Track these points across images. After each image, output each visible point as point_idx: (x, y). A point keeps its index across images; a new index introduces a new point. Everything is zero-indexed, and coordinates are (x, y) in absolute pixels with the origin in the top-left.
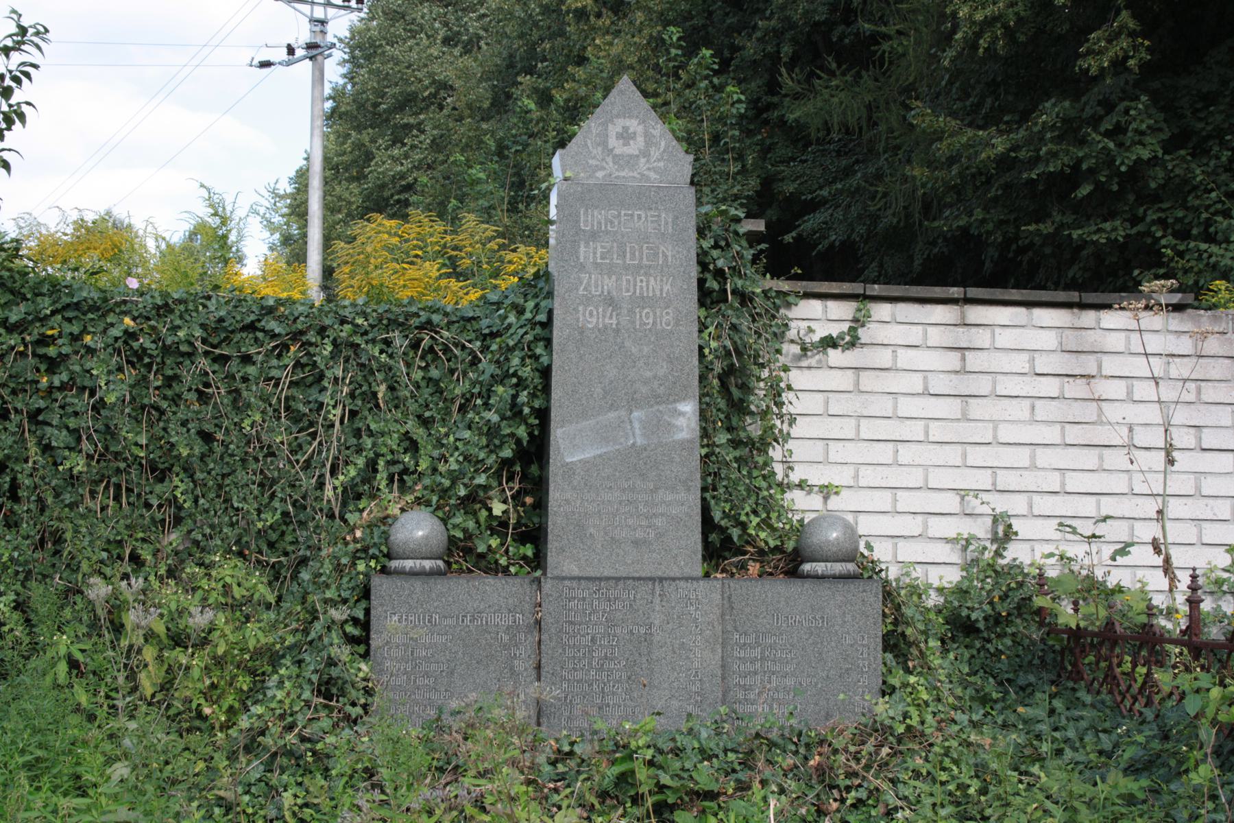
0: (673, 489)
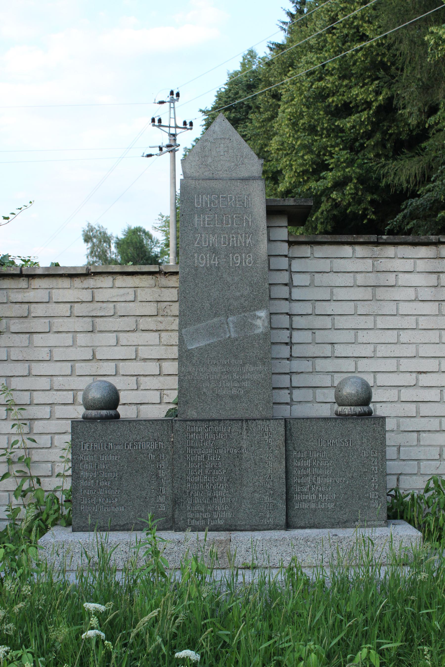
0: (255, 364)
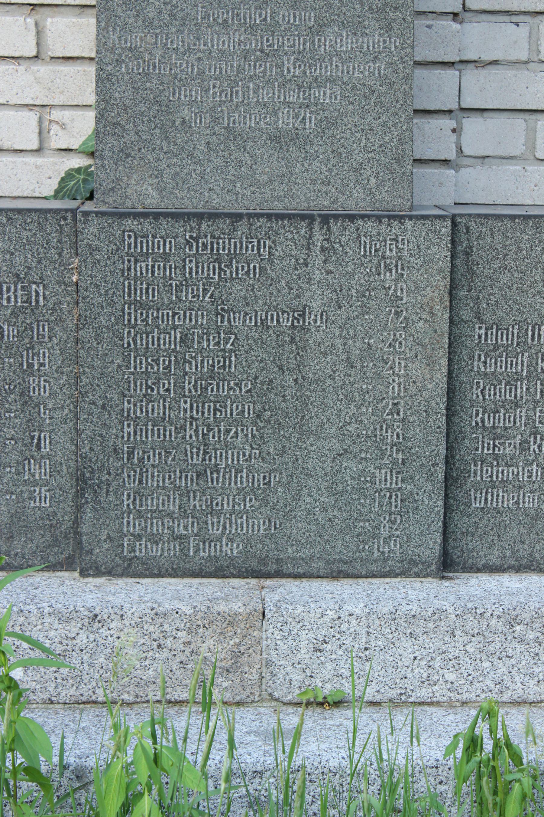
0: (357, 28)
